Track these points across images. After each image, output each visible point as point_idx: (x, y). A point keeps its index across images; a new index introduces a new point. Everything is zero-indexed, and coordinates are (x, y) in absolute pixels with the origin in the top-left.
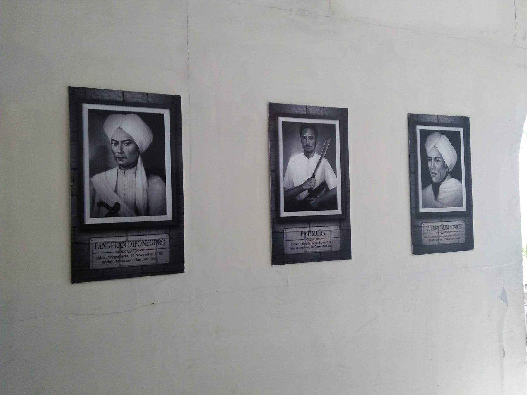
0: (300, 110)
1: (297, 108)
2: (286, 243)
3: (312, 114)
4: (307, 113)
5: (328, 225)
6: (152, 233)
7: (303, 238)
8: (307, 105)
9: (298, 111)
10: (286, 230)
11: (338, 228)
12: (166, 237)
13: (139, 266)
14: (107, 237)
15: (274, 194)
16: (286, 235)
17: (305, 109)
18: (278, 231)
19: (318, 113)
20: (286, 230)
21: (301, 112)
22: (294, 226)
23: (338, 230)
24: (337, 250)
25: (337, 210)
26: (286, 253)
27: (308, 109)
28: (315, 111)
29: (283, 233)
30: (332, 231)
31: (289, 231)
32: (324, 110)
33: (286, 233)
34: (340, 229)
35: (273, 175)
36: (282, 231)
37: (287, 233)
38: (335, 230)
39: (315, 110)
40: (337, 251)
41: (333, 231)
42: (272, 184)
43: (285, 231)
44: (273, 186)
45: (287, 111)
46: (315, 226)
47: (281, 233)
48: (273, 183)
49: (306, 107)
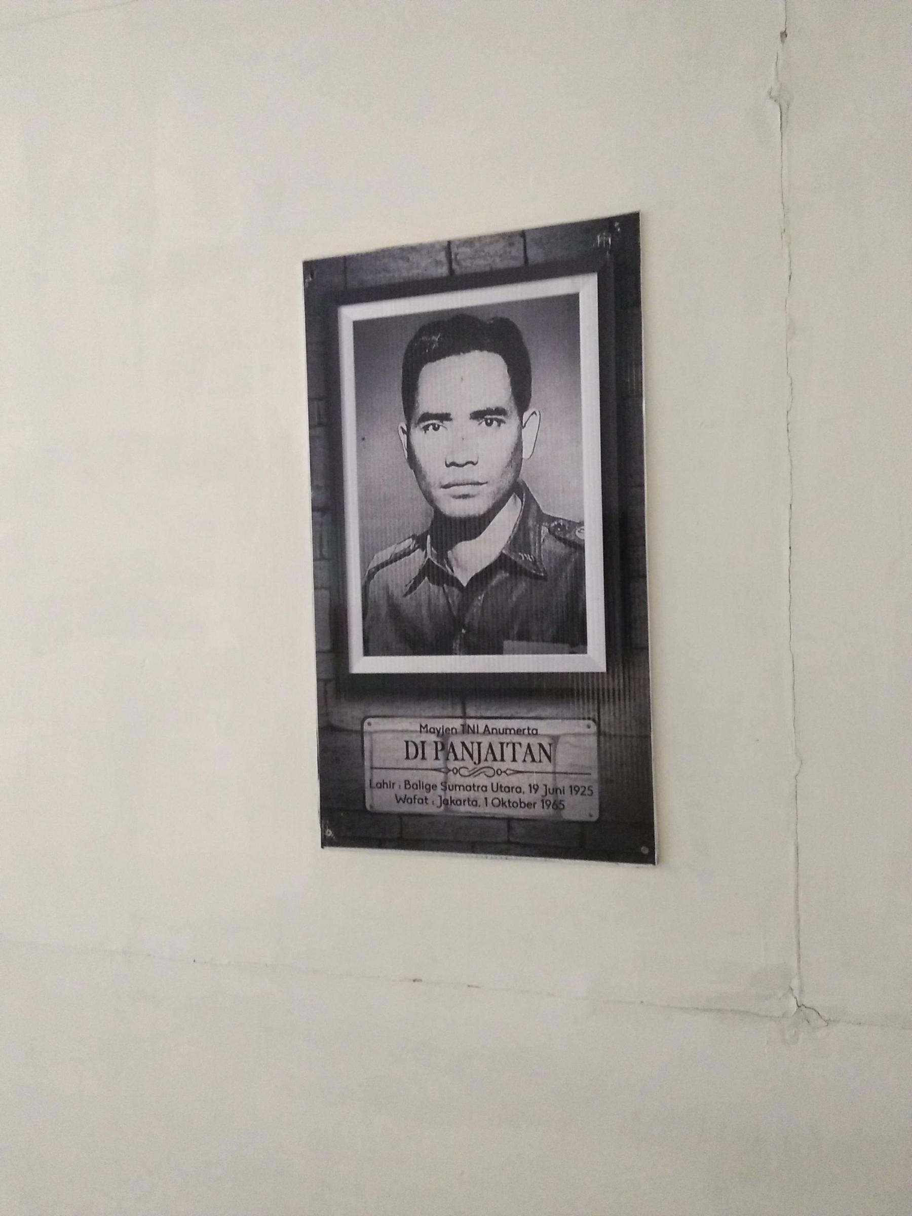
0: (423, 264)
2: (479, 774)
4: (451, 271)
5: (543, 714)
6: (539, 712)
10: (369, 724)
11: (589, 727)
12: (587, 730)
13: (503, 819)
14: (407, 717)
15: (326, 593)
16: (371, 740)
17: (442, 256)
18: (343, 725)
19: (498, 260)
20: (369, 724)
22: (401, 712)
23: (589, 734)
24: (584, 817)
25: (586, 653)
26: (371, 807)
27: (456, 255)
28: (483, 254)
29: (361, 733)
30: (561, 739)
31: (381, 727)
33: (371, 733)
35: (321, 525)
36: (359, 728)
37: (375, 736)
38: (575, 735)
40: (582, 824)
41: (572, 740)
42: (318, 556)
43: (366, 727)
45: (370, 279)
47: (356, 732)
48: (321, 554)
49: (448, 246)
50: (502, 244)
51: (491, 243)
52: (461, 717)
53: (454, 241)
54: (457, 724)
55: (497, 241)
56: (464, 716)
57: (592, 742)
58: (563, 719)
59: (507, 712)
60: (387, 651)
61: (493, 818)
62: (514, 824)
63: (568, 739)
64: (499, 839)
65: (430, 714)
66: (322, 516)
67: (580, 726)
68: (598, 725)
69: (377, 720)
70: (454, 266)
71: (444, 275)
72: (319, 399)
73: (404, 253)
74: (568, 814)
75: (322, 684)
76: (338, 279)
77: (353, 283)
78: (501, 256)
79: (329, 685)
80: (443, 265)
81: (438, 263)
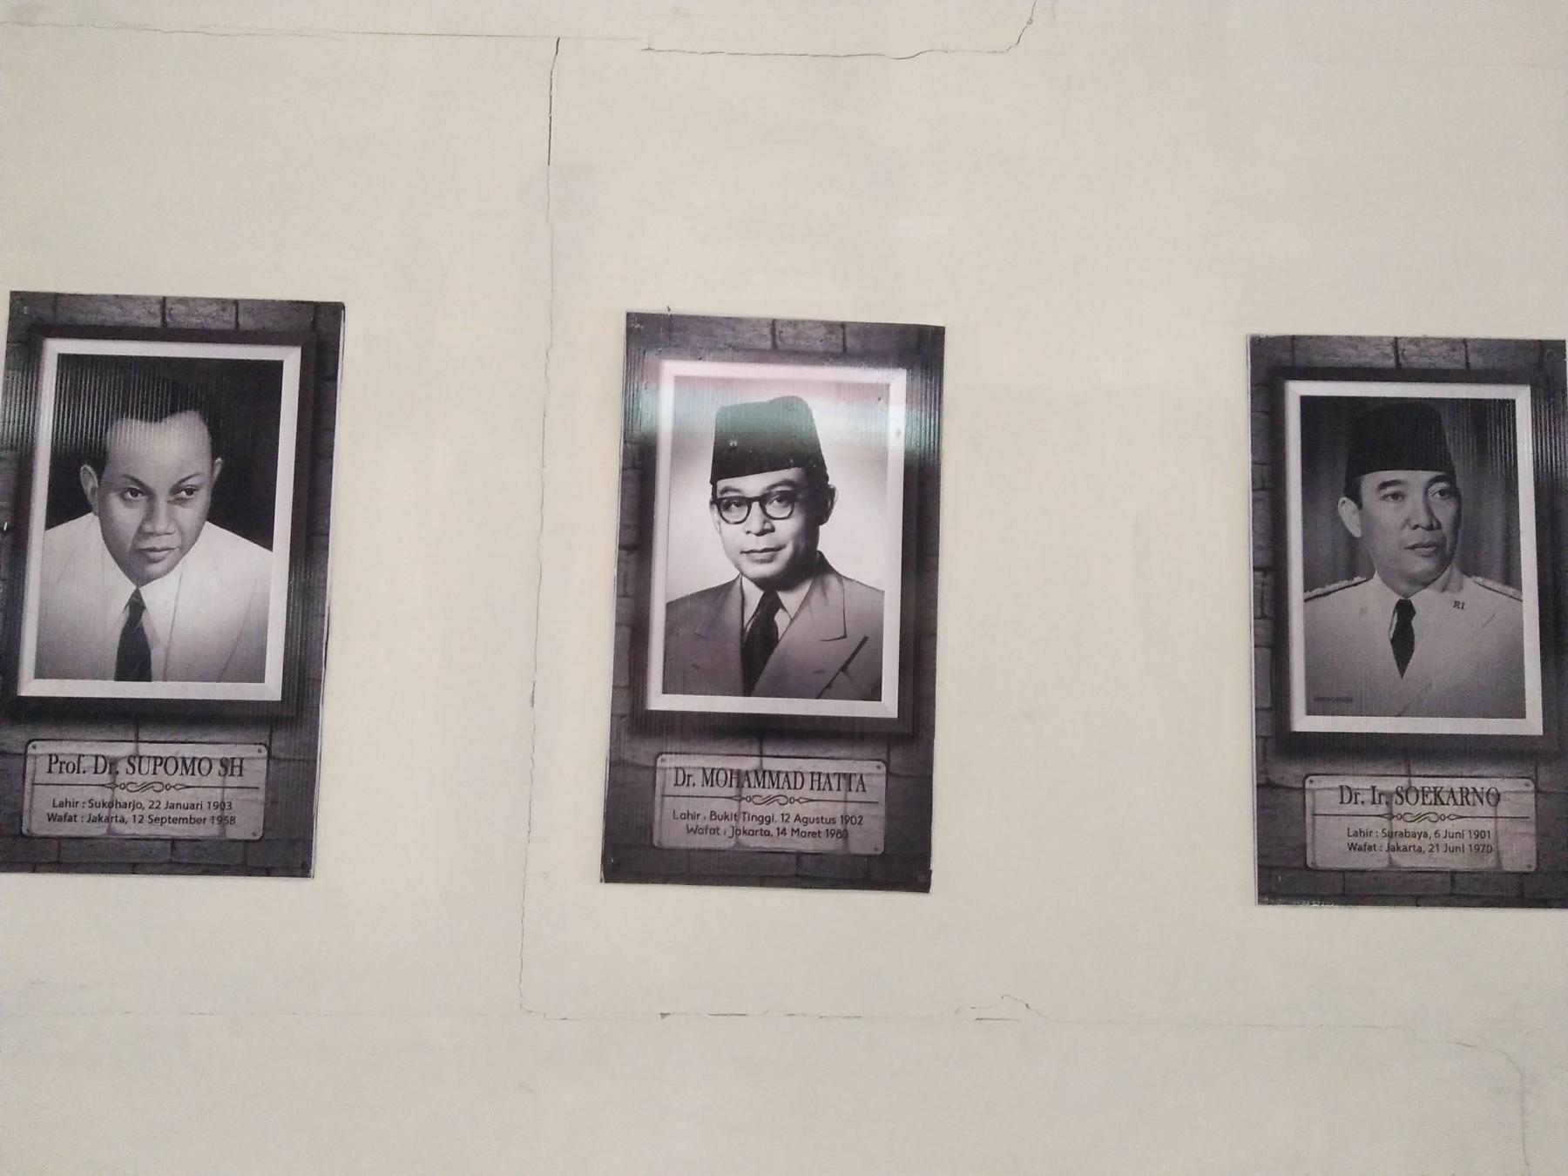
1: (1356, 348)
3: (1415, 366)
5: (1485, 773)
7: (1382, 809)
8: (1398, 334)
9: (1362, 359)
11: (1527, 785)
19: (1442, 361)
21: (1375, 363)
32: (1466, 351)
34: (1537, 791)
35: (1263, 584)
38: (1516, 792)
39: (1433, 350)
41: (1512, 797)
42: (1259, 614)
44: (1261, 622)
45: (1319, 360)
46: (1432, 773)
50: (1445, 347)
51: (1435, 346)
52: (1405, 776)
53: (778, 320)
54: (1403, 782)
55: (1441, 345)
56: (761, 755)
57: (1530, 799)
58: (1503, 777)
59: (1452, 771)
60: (686, 690)
61: (1436, 872)
62: (1457, 877)
63: (1508, 796)
64: (787, 874)
65: (1374, 773)
66: (1264, 576)
67: (1519, 784)
68: (1536, 782)
69: (669, 756)
70: (1401, 360)
71: (1392, 366)
72: (1264, 464)
73: (1354, 342)
74: (1508, 866)
75: (1260, 741)
76: (1286, 356)
77: (1301, 361)
78: (1444, 358)
79: (1270, 741)
80: (1390, 358)
81: (1386, 356)
